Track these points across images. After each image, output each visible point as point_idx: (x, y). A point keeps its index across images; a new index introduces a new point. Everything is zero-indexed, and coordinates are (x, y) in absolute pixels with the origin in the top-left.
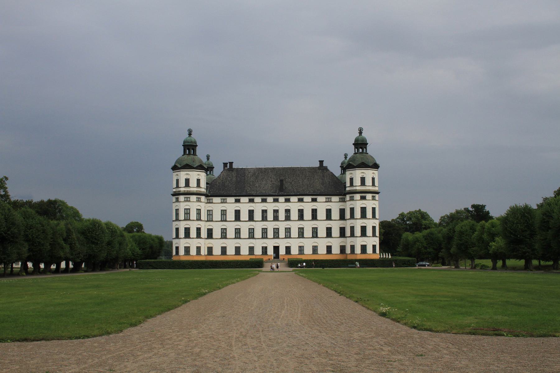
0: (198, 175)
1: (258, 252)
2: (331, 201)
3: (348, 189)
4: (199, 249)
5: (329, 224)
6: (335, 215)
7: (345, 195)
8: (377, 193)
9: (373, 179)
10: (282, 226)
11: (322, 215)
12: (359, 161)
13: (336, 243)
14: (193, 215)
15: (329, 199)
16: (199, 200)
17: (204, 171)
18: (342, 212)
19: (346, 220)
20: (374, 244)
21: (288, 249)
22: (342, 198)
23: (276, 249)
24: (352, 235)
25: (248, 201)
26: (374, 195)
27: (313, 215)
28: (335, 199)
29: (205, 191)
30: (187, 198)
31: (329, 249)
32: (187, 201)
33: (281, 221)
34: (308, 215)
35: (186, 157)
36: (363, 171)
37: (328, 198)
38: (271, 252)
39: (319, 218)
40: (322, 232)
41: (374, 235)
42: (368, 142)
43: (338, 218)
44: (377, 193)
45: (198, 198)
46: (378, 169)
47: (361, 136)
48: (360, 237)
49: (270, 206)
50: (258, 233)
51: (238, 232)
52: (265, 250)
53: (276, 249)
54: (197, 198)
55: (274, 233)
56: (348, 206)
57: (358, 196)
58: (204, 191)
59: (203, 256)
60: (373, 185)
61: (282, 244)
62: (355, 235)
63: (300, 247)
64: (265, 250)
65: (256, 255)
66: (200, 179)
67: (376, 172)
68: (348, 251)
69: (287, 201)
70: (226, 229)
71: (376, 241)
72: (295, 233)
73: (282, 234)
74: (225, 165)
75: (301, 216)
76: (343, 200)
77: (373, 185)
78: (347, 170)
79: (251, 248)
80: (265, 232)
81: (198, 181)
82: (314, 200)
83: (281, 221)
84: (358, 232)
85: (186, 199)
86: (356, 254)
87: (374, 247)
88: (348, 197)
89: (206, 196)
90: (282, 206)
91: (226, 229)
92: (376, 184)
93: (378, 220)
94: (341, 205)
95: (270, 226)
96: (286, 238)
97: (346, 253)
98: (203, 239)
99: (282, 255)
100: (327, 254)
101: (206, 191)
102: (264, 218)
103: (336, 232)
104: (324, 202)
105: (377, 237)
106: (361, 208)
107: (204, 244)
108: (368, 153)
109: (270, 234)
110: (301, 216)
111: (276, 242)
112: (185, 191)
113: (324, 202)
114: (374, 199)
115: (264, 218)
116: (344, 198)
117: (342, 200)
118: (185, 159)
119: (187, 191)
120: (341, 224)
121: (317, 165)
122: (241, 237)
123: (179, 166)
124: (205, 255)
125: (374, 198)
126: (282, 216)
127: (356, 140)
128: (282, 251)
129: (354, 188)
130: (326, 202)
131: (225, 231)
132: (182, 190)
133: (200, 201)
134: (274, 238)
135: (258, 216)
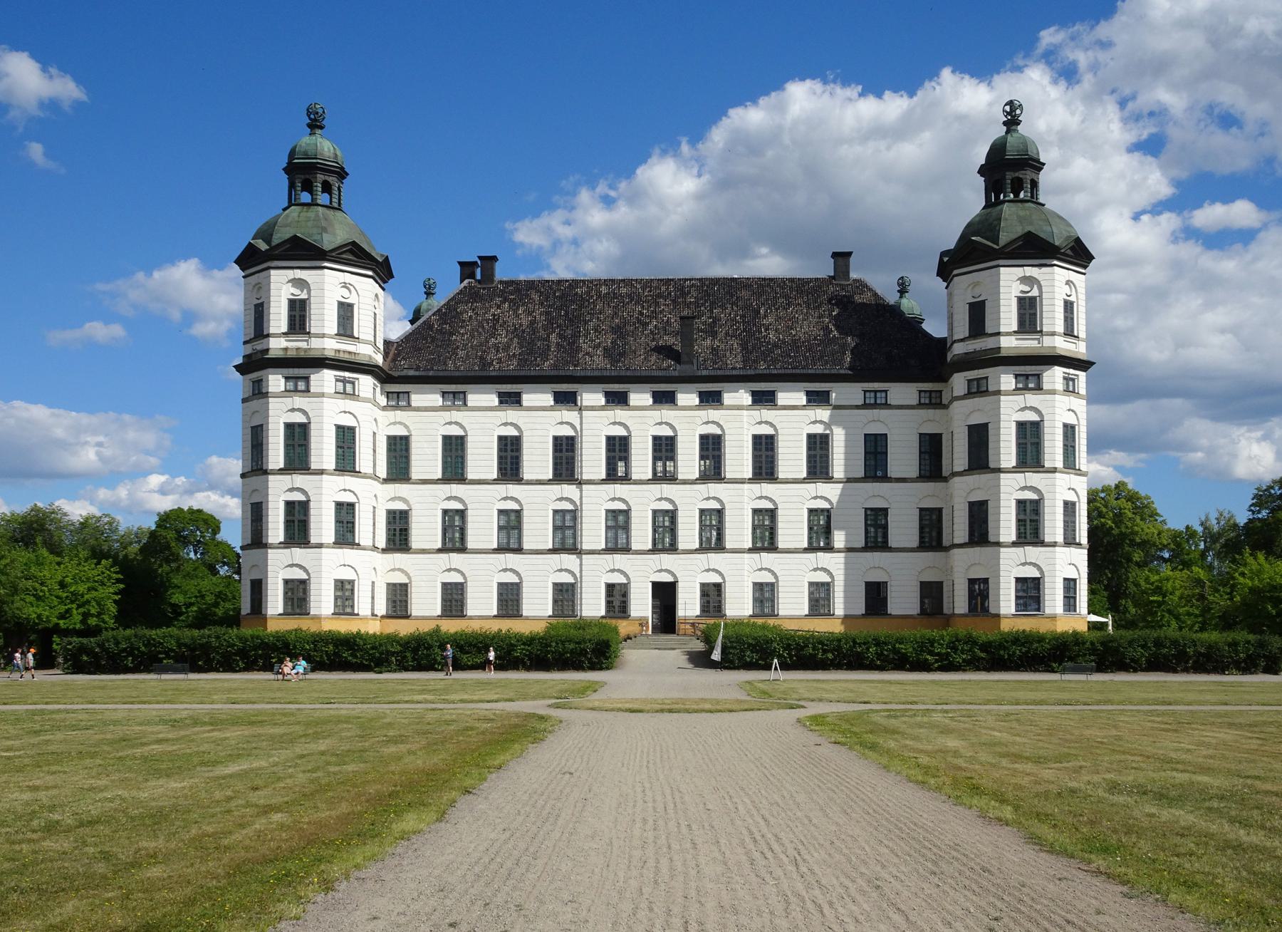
1: (593, 605)
2: (886, 406)
3: (958, 349)
7: (944, 379)
8: (1083, 365)
9: (1069, 306)
12: (1009, 231)
14: (324, 451)
15: (878, 395)
16: (348, 393)
17: (370, 273)
18: (931, 448)
19: (945, 480)
20: (1072, 574)
21: (712, 595)
22: (931, 392)
23: (665, 594)
27: (811, 460)
28: (902, 393)
29: (379, 359)
33: (685, 482)
35: (295, 214)
36: (1029, 271)
37: (876, 392)
38: (642, 605)
41: (1070, 541)
43: (913, 472)
44: (1083, 365)
45: (344, 381)
46: (1085, 267)
47: (1015, 135)
50: (593, 533)
51: (511, 523)
52: (617, 597)
53: (665, 594)
54: (337, 380)
55: (655, 531)
56: (963, 414)
58: (370, 356)
59: (365, 618)
60: (1069, 332)
63: (759, 587)
64: (617, 597)
66: (351, 306)
67: (1079, 279)
68: (960, 603)
72: (739, 531)
73: (688, 534)
74: (467, 269)
76: (935, 402)
77: (1069, 332)
78: (956, 272)
79: (561, 590)
80: (619, 521)
81: (346, 312)
83: (685, 482)
87: (1070, 584)
88: (959, 382)
89: (383, 376)
92: (1081, 328)
93: (1084, 479)
94: (929, 421)
97: (946, 611)
98: (364, 549)
101: (385, 359)
104: (857, 407)
108: (1044, 205)
109: (642, 535)
112: (286, 349)
113: (857, 407)
114: (1071, 389)
116: (941, 391)
117: (930, 398)
118: (290, 220)
119: (298, 349)
120: (927, 495)
121: (825, 269)
122: (526, 546)
123: (263, 246)
124: (373, 615)
125: (1070, 387)
127: (997, 150)
128: (688, 605)
130: (865, 406)
132: (277, 345)
133: (353, 396)
134: (654, 550)
135: (593, 461)
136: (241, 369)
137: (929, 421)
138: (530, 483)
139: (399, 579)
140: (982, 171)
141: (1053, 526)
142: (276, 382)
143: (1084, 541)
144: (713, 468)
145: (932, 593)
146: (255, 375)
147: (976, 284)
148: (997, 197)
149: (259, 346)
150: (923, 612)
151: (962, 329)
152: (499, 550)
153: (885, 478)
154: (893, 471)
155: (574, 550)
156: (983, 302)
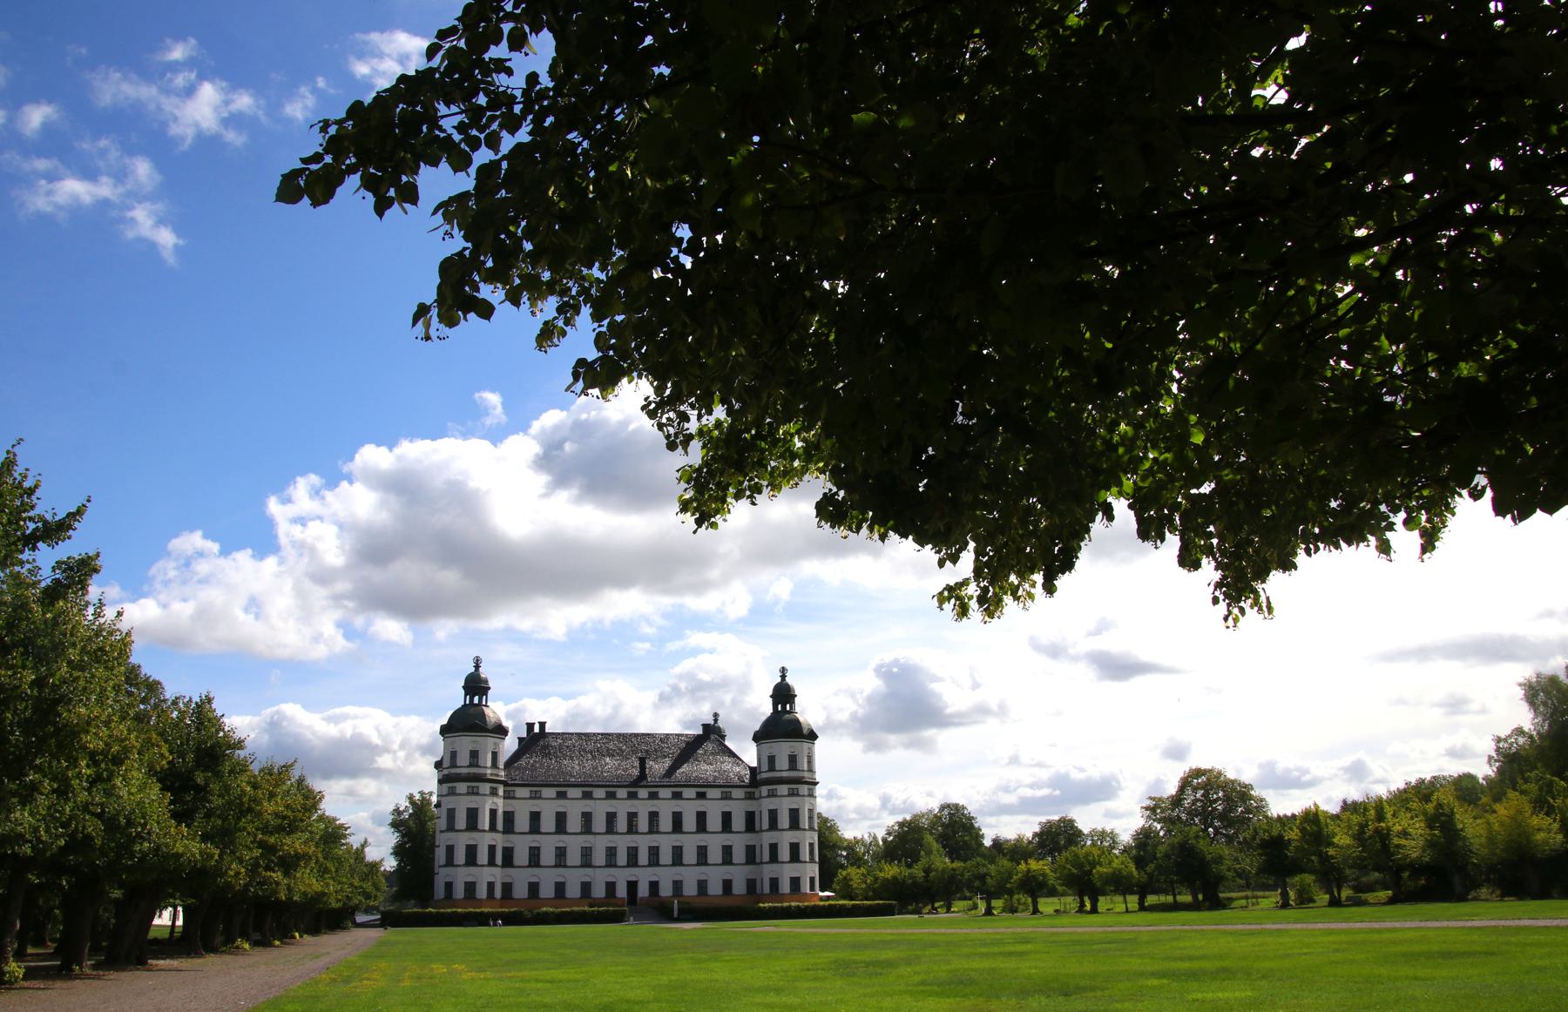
0: (474, 742)
2: (731, 798)
3: (764, 776)
5: (727, 839)
6: (738, 823)
10: (643, 843)
11: (714, 822)
13: (739, 875)
16: (494, 793)
18: (750, 818)
21: (654, 886)
23: (632, 886)
24: (774, 858)
25: (580, 795)
26: (811, 787)
30: (473, 787)
31: (727, 885)
34: (689, 823)
38: (622, 892)
39: (710, 828)
40: (715, 855)
41: (812, 860)
42: (796, 693)
48: (790, 862)
49: (622, 807)
52: (611, 887)
53: (632, 886)
56: (768, 804)
57: (783, 789)
61: (644, 876)
62: (780, 860)
64: (611, 887)
65: (595, 899)
69: (654, 796)
70: (538, 848)
71: (814, 870)
73: (643, 858)
75: (677, 825)
82: (701, 796)
84: (784, 854)
85: (470, 791)
86: (783, 894)
87: (812, 880)
88: (764, 790)
89: (505, 784)
90: (643, 808)
91: (538, 848)
95: (622, 843)
96: (650, 865)
99: (642, 898)
100: (723, 895)
102: (611, 828)
103: (739, 855)
104: (718, 799)
105: (815, 862)
106: (791, 810)
107: (497, 875)
109: (622, 858)
110: (677, 825)
111: (632, 874)
113: (718, 799)
115: (611, 828)
120: (750, 839)
131: (536, 853)
138: (571, 834)
139: (508, 880)
140: (771, 696)
142: (462, 787)
143: (817, 860)
144: (653, 828)
145: (751, 884)
146: (450, 785)
147: (771, 748)
148: (784, 707)
150: (748, 893)
151: (765, 767)
152: (556, 866)
153: (731, 832)
154: (734, 829)
155: (590, 866)
156: (774, 756)
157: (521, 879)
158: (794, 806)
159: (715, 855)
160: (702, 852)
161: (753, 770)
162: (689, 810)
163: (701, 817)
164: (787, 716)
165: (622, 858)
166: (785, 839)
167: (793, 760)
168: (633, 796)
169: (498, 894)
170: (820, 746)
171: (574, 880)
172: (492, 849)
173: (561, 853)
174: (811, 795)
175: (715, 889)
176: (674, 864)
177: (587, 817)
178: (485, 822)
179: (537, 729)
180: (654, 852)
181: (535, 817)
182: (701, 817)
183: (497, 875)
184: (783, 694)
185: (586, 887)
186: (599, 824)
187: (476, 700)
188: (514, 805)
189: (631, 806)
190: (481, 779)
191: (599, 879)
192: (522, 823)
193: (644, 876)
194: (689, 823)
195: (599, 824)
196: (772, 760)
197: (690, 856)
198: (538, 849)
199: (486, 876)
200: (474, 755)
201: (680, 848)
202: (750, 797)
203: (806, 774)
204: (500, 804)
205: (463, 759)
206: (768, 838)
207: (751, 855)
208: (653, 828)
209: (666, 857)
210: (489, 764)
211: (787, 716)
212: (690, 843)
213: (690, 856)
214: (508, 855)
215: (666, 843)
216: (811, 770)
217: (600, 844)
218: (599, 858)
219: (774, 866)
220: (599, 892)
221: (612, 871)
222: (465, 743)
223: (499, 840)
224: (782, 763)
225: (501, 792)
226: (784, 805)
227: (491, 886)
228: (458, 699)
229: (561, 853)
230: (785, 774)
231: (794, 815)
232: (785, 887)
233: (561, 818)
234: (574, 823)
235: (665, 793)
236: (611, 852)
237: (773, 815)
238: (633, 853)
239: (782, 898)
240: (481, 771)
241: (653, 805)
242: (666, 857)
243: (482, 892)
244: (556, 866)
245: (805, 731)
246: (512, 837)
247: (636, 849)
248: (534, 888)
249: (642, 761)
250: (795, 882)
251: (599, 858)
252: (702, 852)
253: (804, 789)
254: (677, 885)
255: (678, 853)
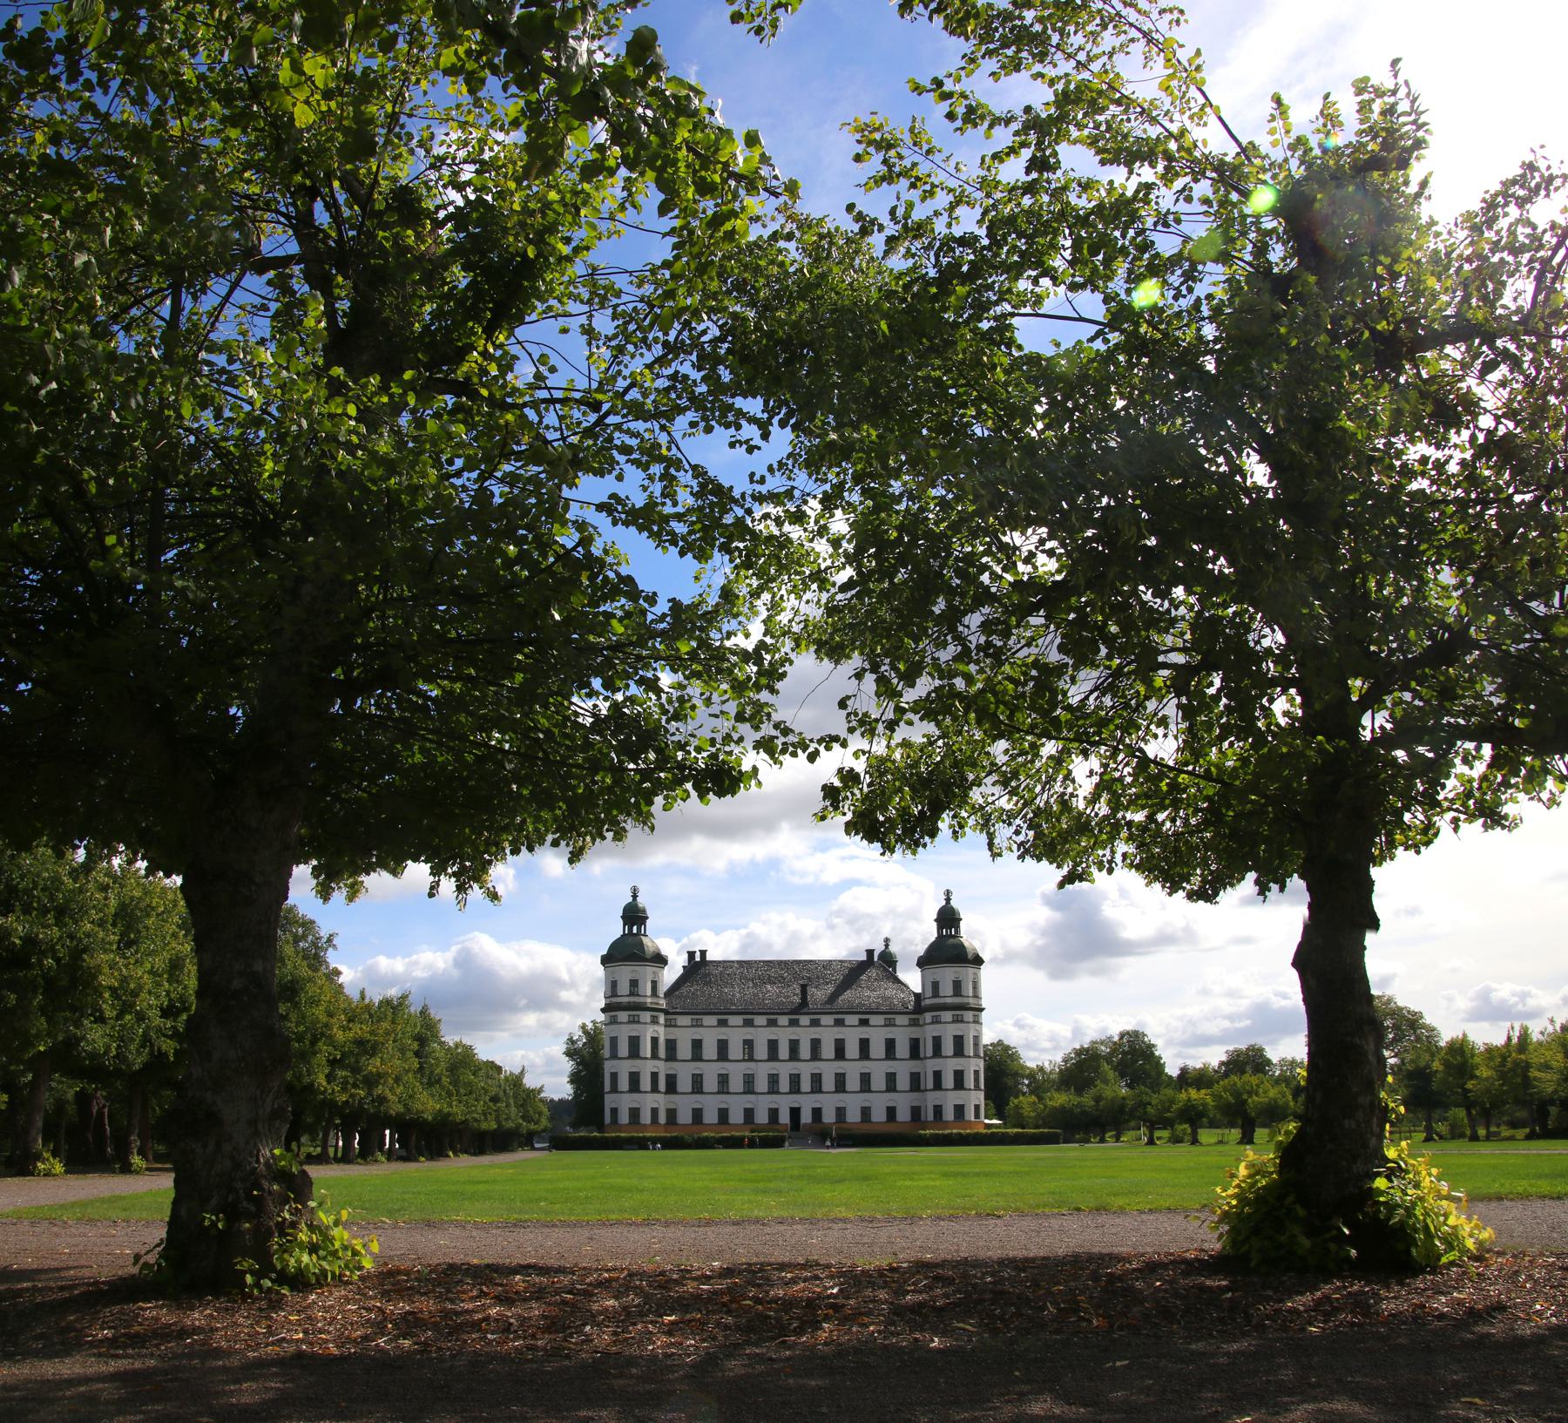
3: (928, 1002)
4: (655, 1112)
5: (890, 1066)
6: (902, 1050)
10: (806, 1070)
11: (878, 1049)
13: (903, 1103)
16: (655, 1021)
18: (915, 1047)
21: (817, 1113)
24: (938, 1085)
27: (861, 1050)
31: (891, 1112)
32: (634, 1022)
34: (852, 1050)
38: (785, 1118)
40: (878, 1082)
41: (977, 1088)
43: (907, 1055)
49: (784, 1035)
52: (774, 1113)
56: (931, 1031)
57: (947, 1016)
61: (807, 1103)
64: (774, 1113)
69: (815, 1023)
71: (979, 1097)
73: (806, 1085)
75: (840, 1053)
82: (864, 1023)
84: (948, 1081)
87: (977, 1107)
88: (928, 1016)
89: (666, 1012)
90: (805, 1035)
94: (915, 1032)
95: (784, 1070)
103: (903, 1082)
107: (661, 1101)
109: (784, 1085)
110: (840, 1053)
120: (914, 1066)
126: (805, 1051)
128: (806, 1117)
129: (941, 1001)
136: (603, 1010)
137: (915, 1032)
139: (671, 1106)
141: (969, 1081)
142: (623, 1016)
144: (816, 1055)
145: (916, 1112)
149: (614, 1000)
151: (929, 993)
157: (685, 1106)
158: (959, 1033)
159: (878, 1082)
160: (865, 1080)
161: (917, 996)
162: (852, 1037)
163: (864, 1045)
164: (951, 941)
165: (784, 1085)
166: (949, 1066)
167: (957, 986)
168: (794, 1023)
169: (662, 1119)
170: (985, 973)
171: (737, 1107)
172: (655, 1076)
173: (723, 1080)
174: (977, 1022)
175: (879, 1116)
176: (837, 1091)
177: (749, 1044)
178: (647, 1050)
179: (698, 958)
180: (817, 1080)
181: (697, 1045)
182: (864, 1045)
183: (661, 1101)
184: (948, 918)
185: (749, 1114)
186: (761, 1051)
187: (635, 930)
188: (675, 1033)
189: (793, 1033)
190: (642, 1007)
191: (761, 1107)
192: (684, 1051)
193: (807, 1103)
194: (852, 1050)
195: (761, 1051)
196: (936, 986)
197: (853, 1083)
198: (701, 1075)
199: (649, 1102)
200: (634, 983)
201: (843, 1075)
202: (914, 1023)
203: (971, 1001)
204: (661, 1032)
205: (624, 988)
206: (932, 1065)
207: (916, 1082)
208: (816, 1055)
209: (828, 1083)
210: (649, 993)
211: (951, 941)
212: (853, 1070)
213: (853, 1083)
214: (672, 1083)
215: (828, 1070)
216: (976, 996)
217: (762, 1071)
218: (762, 1084)
219: (938, 1094)
220: (762, 1118)
221: (774, 1097)
222: (625, 973)
223: (662, 1068)
224: (947, 989)
225: (662, 1019)
226: (948, 1032)
227: (655, 1112)
228: (616, 929)
229: (723, 1080)
230: (949, 1000)
231: (959, 1041)
232: (949, 1115)
233: (723, 1046)
234: (735, 1051)
235: (827, 1020)
236: (773, 1080)
237: (937, 1042)
238: (795, 1080)
239: (946, 1124)
240: (641, 1000)
241: (815, 1033)
242: (828, 1083)
243: (646, 1118)
244: (718, 1093)
245: (970, 956)
246: (675, 1064)
247: (798, 1076)
248: (697, 1114)
249: (804, 988)
250: (960, 1110)
251: (762, 1084)
252: (865, 1080)
253: (969, 1015)
254: (841, 1112)
255: (840, 1081)
